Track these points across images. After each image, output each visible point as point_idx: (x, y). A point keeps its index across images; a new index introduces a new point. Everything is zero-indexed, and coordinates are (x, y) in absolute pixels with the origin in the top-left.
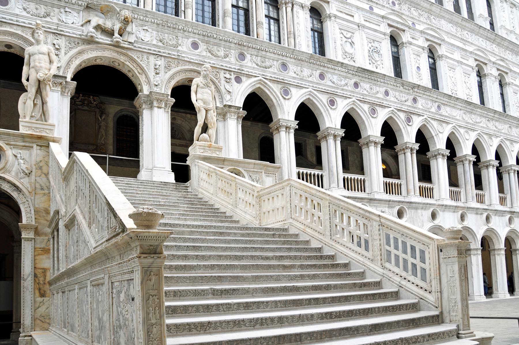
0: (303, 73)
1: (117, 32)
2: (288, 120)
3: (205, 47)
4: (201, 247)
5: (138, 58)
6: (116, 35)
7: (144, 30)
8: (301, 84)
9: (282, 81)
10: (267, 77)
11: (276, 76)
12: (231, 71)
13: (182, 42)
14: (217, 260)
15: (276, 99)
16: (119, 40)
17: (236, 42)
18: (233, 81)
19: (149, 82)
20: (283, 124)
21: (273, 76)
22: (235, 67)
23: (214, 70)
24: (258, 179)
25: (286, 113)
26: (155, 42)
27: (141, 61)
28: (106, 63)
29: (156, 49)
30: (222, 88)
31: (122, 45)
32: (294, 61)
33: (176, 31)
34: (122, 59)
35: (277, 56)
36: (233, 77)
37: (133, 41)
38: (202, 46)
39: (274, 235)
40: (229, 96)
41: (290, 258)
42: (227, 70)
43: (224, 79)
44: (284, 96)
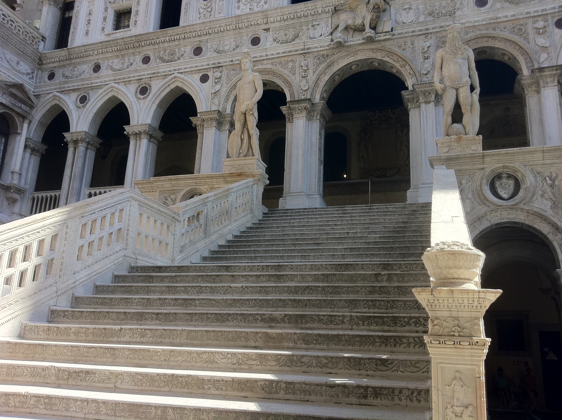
1: (368, 25)
4: (195, 299)
5: (400, 47)
7: (405, 9)
12: (547, 14)
13: (461, 3)
14: (187, 320)
22: (553, 6)
24: (554, 175)
26: (422, 19)
27: (404, 50)
29: (422, 28)
31: (376, 39)
36: (551, 22)
39: (377, 275)
41: (320, 321)
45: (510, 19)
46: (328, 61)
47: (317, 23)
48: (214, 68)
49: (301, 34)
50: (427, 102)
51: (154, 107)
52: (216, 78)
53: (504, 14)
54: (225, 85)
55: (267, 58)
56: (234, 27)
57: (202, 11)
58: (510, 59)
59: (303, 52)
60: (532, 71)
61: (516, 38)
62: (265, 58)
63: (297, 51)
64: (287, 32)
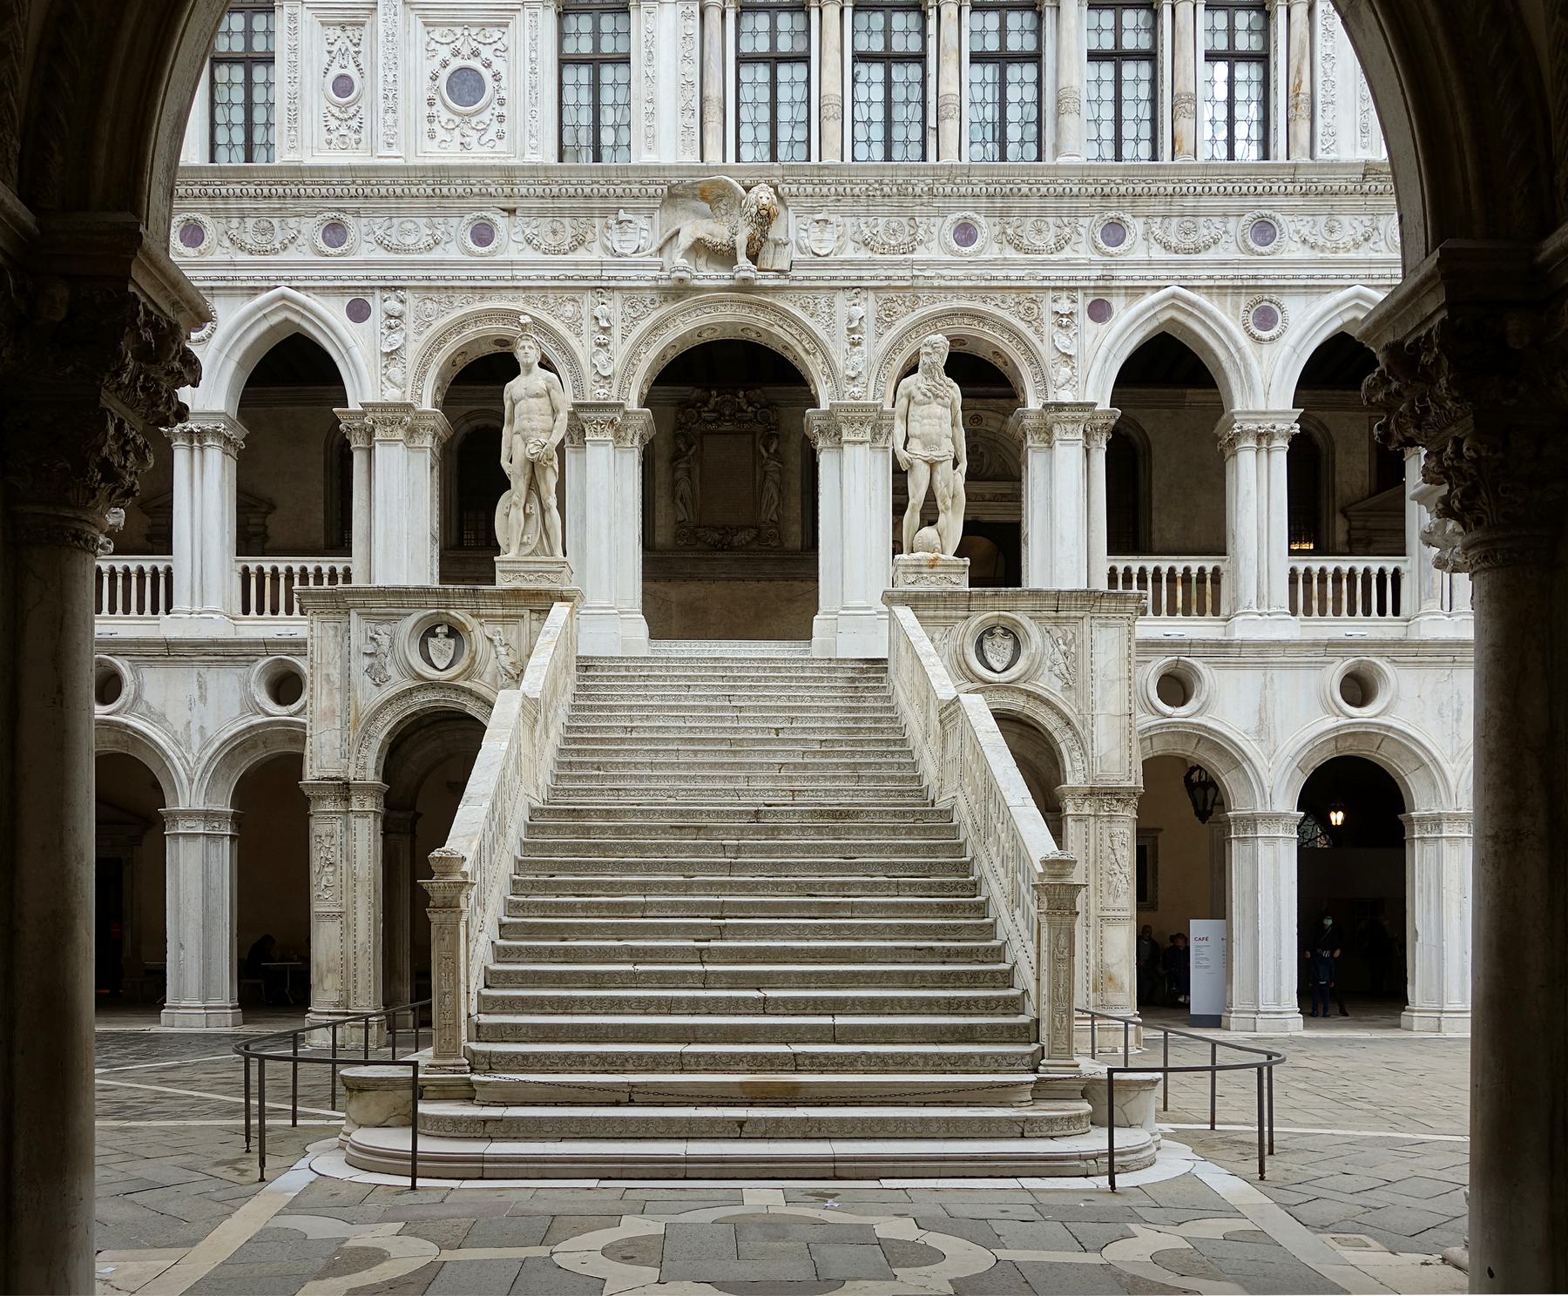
0: (1335, 236)
2: (1264, 413)
3: (997, 230)
5: (804, 308)
6: (743, 260)
8: (1324, 277)
9: (1251, 283)
10: (1196, 283)
11: (1230, 273)
12: (1076, 288)
15: (1227, 348)
16: (748, 274)
17: (1091, 190)
18: (1083, 318)
19: (832, 373)
20: (1245, 427)
21: (1217, 273)
22: (1086, 273)
23: (1022, 298)
25: (1260, 389)
26: (849, 253)
27: (812, 315)
28: (729, 335)
30: (1045, 351)
31: (758, 283)
32: (1299, 201)
33: (908, 202)
34: (762, 320)
35: (1236, 202)
37: (786, 266)
38: (986, 227)
40: (1068, 370)
42: (1062, 288)
43: (1053, 319)
44: (1258, 333)
45: (1014, 284)
46: (655, 315)
47: (629, 217)
48: (382, 288)
49: (589, 237)
50: (855, 443)
51: (232, 365)
52: (391, 317)
53: (1004, 273)
54: (412, 336)
55: (515, 284)
56: (429, 191)
57: (333, 123)
58: (1006, 363)
59: (598, 283)
60: (1046, 406)
61: (1022, 326)
62: (510, 284)
63: (585, 278)
64: (556, 225)
